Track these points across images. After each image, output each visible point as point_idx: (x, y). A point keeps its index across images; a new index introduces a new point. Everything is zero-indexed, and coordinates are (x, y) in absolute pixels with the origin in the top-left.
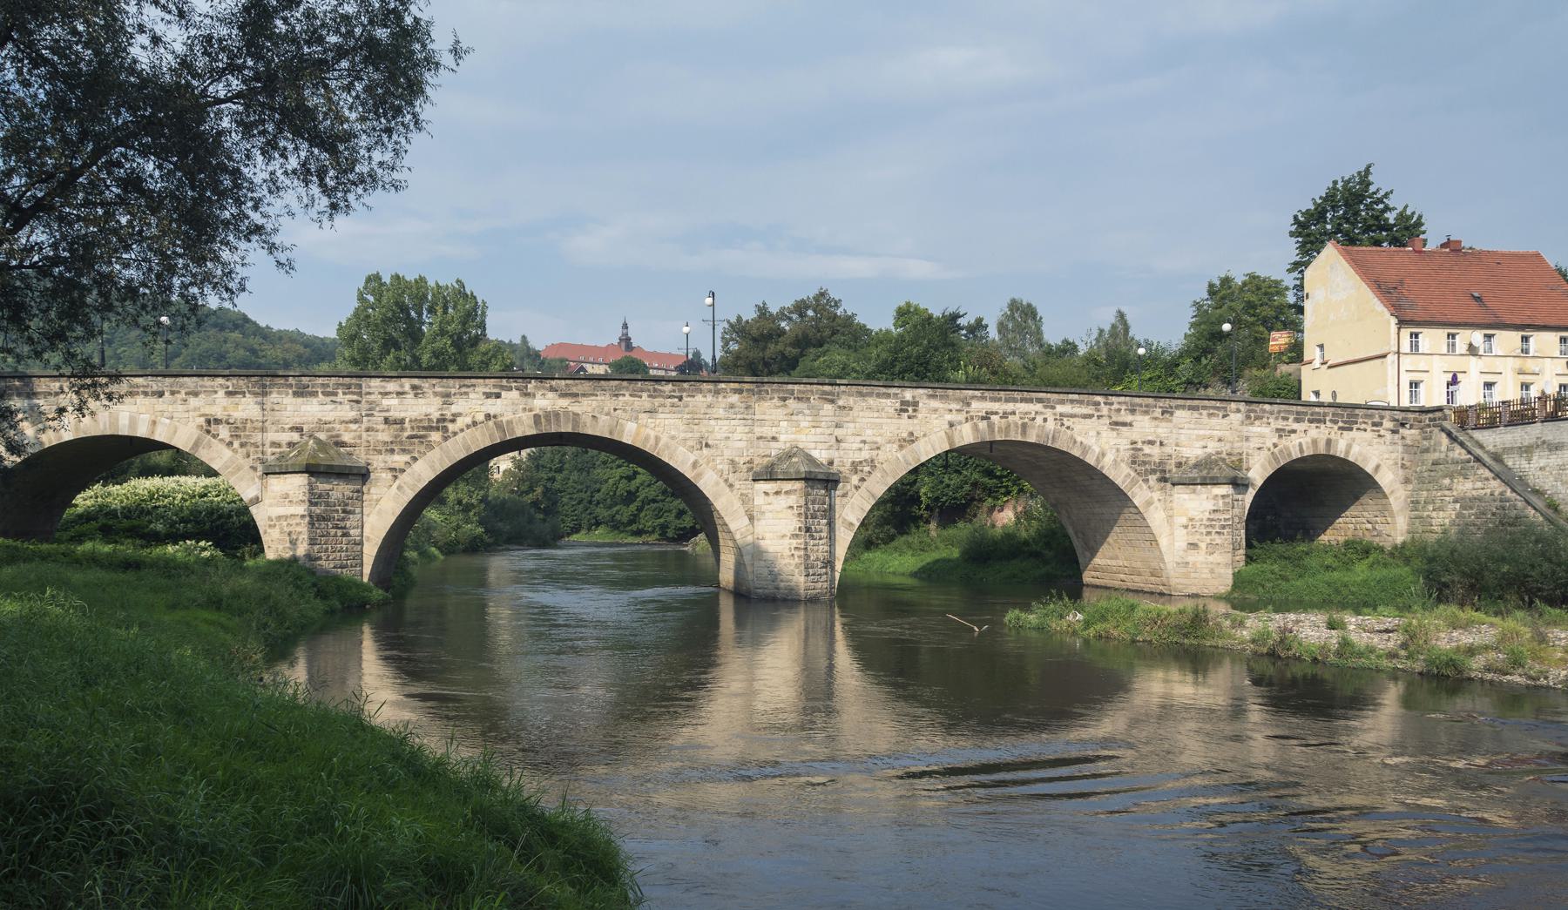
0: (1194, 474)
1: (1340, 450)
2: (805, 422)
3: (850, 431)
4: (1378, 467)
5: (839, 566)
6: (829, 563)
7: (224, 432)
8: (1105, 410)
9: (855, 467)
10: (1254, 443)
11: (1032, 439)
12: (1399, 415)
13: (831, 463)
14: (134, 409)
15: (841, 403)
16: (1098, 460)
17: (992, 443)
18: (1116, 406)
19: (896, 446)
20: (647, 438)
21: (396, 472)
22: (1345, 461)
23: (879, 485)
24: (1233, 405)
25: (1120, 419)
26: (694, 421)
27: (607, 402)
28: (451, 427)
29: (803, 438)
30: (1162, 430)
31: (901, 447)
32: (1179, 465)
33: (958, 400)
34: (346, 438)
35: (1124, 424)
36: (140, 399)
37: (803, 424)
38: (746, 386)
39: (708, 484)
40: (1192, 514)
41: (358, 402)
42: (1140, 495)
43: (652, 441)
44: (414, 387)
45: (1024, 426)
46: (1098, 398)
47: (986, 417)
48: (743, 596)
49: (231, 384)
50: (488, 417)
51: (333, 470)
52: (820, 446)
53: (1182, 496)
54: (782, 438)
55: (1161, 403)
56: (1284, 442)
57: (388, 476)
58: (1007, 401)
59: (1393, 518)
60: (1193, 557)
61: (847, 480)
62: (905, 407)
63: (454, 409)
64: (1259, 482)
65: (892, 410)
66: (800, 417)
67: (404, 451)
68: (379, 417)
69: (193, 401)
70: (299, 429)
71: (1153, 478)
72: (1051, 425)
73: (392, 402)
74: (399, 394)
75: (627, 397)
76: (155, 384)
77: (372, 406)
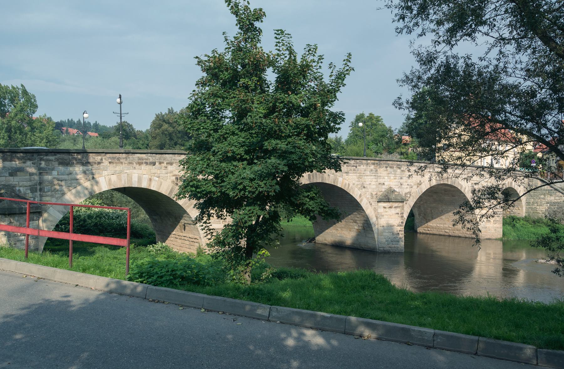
11: (449, 183)
14: (140, 172)
15: (402, 169)
20: (346, 185)
26: (360, 177)
29: (391, 183)
31: (418, 186)
36: (143, 166)
37: (392, 178)
38: (376, 162)
39: (364, 204)
54: (386, 183)
69: (170, 168)
76: (151, 158)
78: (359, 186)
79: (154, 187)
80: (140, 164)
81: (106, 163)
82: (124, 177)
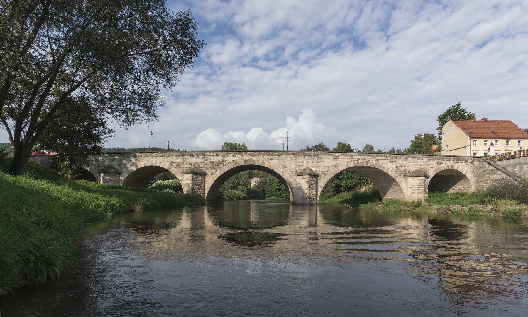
0: (414, 174)
1: (455, 168)
2: (310, 162)
4: (466, 172)
5: (318, 197)
6: (316, 196)
7: (175, 165)
9: (323, 172)
10: (431, 166)
11: (369, 165)
12: (473, 159)
17: (359, 167)
21: (212, 174)
22: (456, 171)
23: (329, 177)
24: (425, 156)
26: (282, 162)
27: (262, 157)
30: (405, 163)
32: (409, 172)
33: (349, 156)
34: (201, 166)
36: (157, 158)
39: (285, 176)
40: (413, 184)
42: (398, 180)
45: (367, 162)
48: (294, 204)
49: (176, 154)
50: (233, 161)
51: (198, 173)
53: (410, 180)
54: (304, 165)
55: (404, 156)
56: (439, 166)
57: (210, 175)
59: (471, 186)
60: (413, 195)
61: (321, 176)
63: (225, 159)
64: (432, 176)
68: (208, 161)
70: (191, 164)
71: (402, 175)
72: (374, 162)
73: (212, 158)
76: (161, 154)
77: (207, 159)
79: (162, 166)
80: (156, 157)
81: (143, 157)
82: (150, 162)
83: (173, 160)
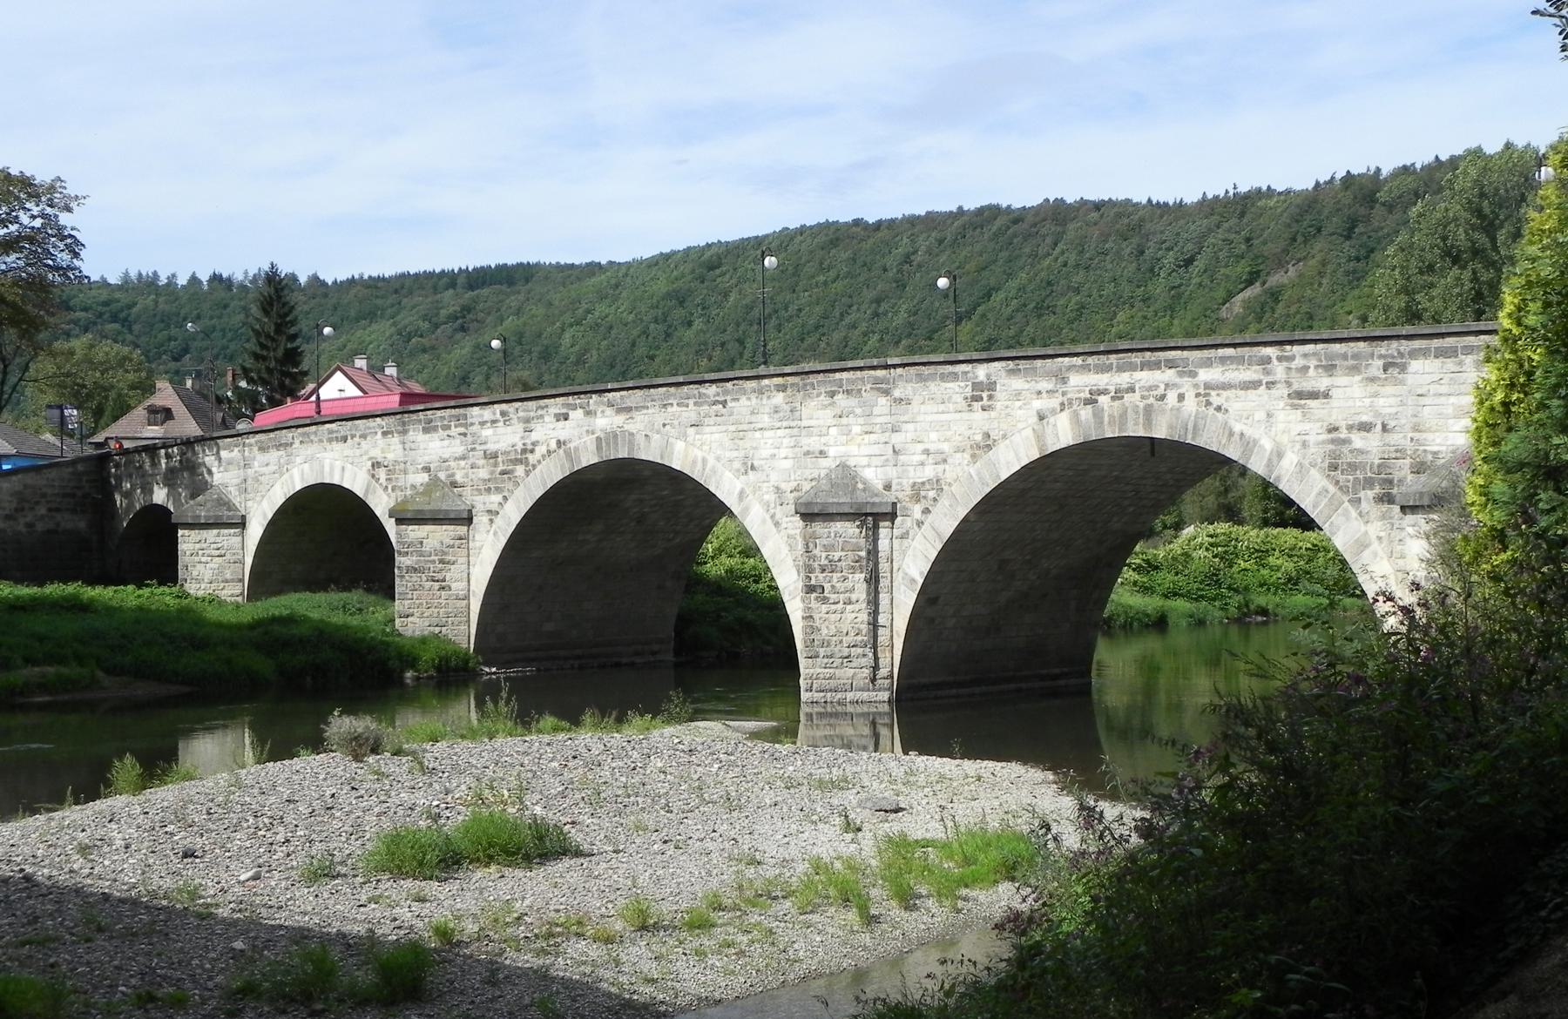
3: (910, 436)
8: (1279, 370)
11: (1160, 432)
13: (888, 487)
15: (897, 393)
16: (1270, 465)
18: (1299, 362)
19: (967, 456)
20: (694, 462)
23: (946, 520)
25: (1307, 385)
28: (532, 458)
30: (1387, 401)
31: (973, 456)
32: (1419, 468)
34: (459, 478)
35: (1314, 395)
37: (856, 429)
38: (790, 379)
41: (465, 435)
43: (699, 465)
44: (503, 414)
45: (1148, 410)
46: (1270, 351)
47: (1090, 401)
50: (559, 442)
52: (876, 461)
54: (832, 452)
55: (1383, 348)
58: (1121, 369)
62: (981, 394)
63: (534, 436)
65: (959, 399)
66: (851, 419)
67: (497, 489)
72: (1191, 405)
73: (487, 432)
74: (494, 422)
75: (675, 408)
78: (737, 465)
80: (330, 440)
83: (377, 453)
